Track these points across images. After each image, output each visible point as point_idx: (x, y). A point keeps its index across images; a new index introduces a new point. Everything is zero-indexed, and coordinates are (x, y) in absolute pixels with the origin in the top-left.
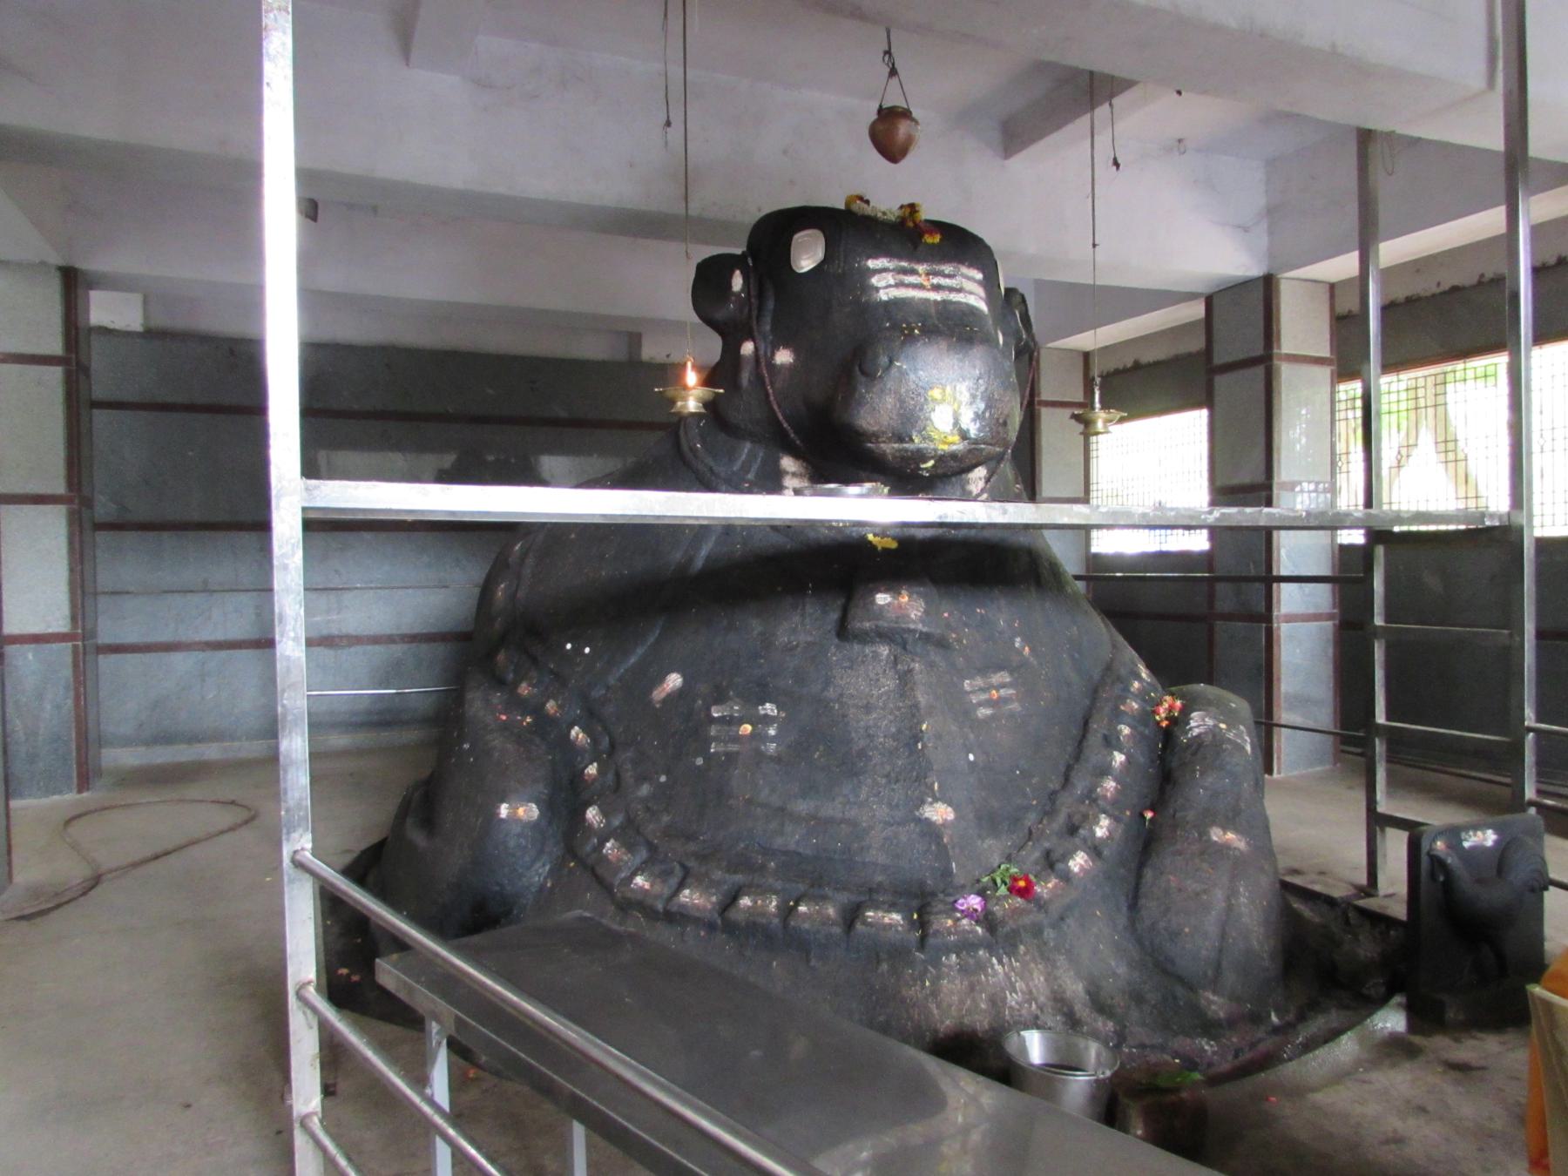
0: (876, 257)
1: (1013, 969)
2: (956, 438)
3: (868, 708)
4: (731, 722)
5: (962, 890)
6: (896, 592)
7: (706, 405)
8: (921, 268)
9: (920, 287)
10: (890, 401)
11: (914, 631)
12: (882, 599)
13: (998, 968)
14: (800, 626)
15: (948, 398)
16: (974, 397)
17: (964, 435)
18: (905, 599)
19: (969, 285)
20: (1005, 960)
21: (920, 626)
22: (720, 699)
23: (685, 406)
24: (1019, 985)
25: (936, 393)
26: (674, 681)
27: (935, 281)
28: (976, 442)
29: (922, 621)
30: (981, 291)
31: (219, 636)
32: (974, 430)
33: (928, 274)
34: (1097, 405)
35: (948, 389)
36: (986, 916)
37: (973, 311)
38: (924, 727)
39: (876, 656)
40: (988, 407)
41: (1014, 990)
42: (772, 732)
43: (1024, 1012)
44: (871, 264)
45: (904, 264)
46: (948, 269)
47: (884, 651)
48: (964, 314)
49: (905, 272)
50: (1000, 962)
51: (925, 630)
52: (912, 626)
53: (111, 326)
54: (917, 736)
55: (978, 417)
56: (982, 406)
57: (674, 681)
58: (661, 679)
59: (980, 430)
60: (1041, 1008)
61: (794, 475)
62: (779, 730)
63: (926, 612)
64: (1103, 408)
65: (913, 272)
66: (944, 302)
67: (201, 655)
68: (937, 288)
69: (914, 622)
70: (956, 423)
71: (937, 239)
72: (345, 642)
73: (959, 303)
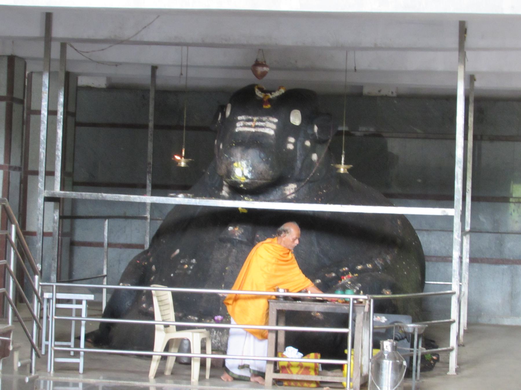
0: (240, 115)
1: (219, 334)
2: (244, 178)
3: (217, 262)
4: (184, 264)
5: (218, 314)
6: (235, 226)
7: (187, 163)
8: (255, 119)
9: (250, 126)
10: (224, 167)
11: (236, 239)
12: (231, 228)
13: (215, 333)
14: (209, 236)
15: (240, 166)
16: (247, 166)
17: (247, 177)
18: (237, 229)
19: (268, 124)
20: (218, 332)
21: (238, 238)
22: (184, 258)
23: (181, 164)
24: (218, 338)
25: (235, 164)
26: (178, 251)
27: (257, 124)
28: (251, 179)
29: (239, 237)
30: (274, 127)
31: (128, 241)
32: (249, 176)
33: (258, 121)
34: (343, 162)
35: (239, 163)
36: (247, 332)
37: (264, 135)
38: (227, 268)
39: (226, 246)
40: (253, 169)
41: (215, 339)
42: (191, 268)
43: (216, 345)
44: (239, 118)
45: (250, 118)
46: (264, 119)
47: (229, 245)
48: (259, 136)
49: (249, 120)
50: (216, 333)
51: (240, 239)
52: (234, 238)
53: (92, 86)
54: (225, 271)
55: (250, 172)
56: (251, 168)
57: (178, 251)
58: (175, 251)
59: (252, 176)
60: (222, 345)
61: (226, 186)
62: (193, 268)
63: (243, 234)
64: (345, 164)
65: (252, 120)
66: (256, 132)
67: (119, 250)
68: (256, 127)
69: (236, 236)
70: (243, 174)
71: (269, 106)
72: (67, 230)
73: (261, 132)
